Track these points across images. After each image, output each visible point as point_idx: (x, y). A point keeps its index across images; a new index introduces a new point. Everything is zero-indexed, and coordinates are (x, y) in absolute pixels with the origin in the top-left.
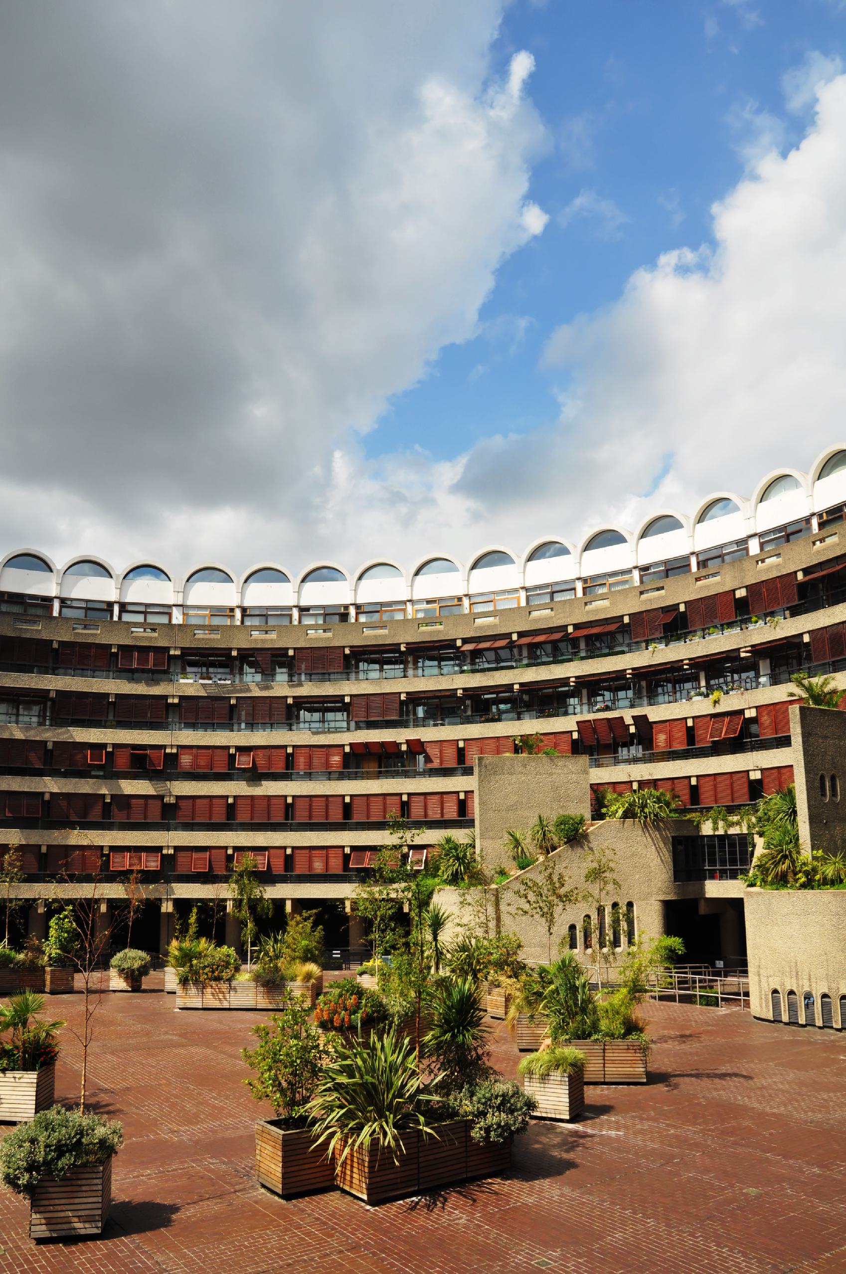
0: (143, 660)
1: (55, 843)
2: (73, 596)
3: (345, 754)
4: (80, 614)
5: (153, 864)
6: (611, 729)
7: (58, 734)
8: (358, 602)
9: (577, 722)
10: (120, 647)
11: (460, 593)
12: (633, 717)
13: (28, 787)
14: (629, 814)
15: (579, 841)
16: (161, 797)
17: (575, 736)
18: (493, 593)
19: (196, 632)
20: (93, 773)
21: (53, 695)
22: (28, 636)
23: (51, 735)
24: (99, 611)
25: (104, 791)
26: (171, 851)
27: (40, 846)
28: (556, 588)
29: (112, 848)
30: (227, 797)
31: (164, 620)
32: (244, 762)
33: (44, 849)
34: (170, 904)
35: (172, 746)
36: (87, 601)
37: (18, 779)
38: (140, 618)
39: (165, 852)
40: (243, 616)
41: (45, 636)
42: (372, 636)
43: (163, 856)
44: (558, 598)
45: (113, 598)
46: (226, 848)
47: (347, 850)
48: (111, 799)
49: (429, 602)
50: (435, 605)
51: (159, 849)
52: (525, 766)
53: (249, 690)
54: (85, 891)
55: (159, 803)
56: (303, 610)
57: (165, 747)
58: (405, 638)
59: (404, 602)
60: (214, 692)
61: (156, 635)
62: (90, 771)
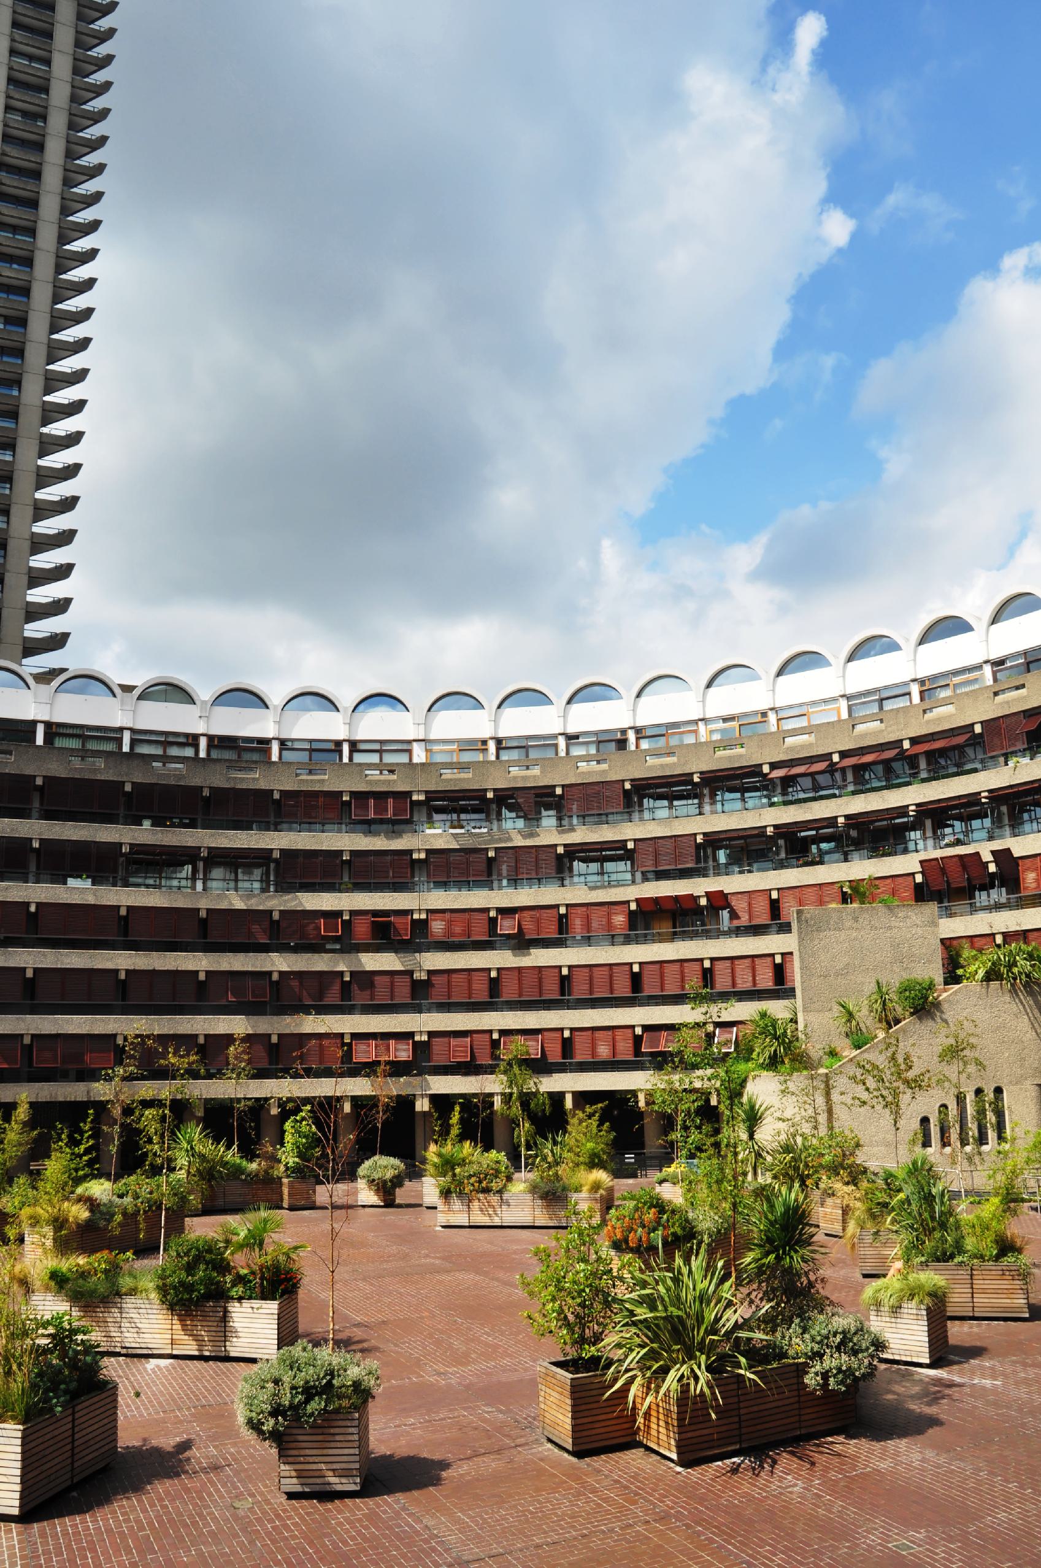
0: (381, 809)
1: (287, 1031)
2: (294, 736)
3: (631, 913)
4: (304, 757)
5: (404, 1053)
6: (964, 867)
9: (921, 862)
10: (353, 794)
11: (763, 706)
12: (993, 852)
14: (992, 975)
15: (929, 1011)
17: (919, 878)
19: (442, 771)
20: (328, 946)
21: (276, 855)
23: (277, 903)
24: (326, 751)
25: (342, 967)
26: (425, 1038)
27: (269, 1035)
28: (885, 694)
29: (355, 1036)
30: (489, 970)
31: (403, 759)
32: (507, 927)
33: (274, 1039)
34: (426, 1101)
36: (311, 741)
38: (374, 758)
39: (417, 1038)
40: (499, 749)
41: (263, 785)
42: (656, 766)
43: (415, 1043)
44: (888, 706)
45: (340, 737)
46: (490, 1032)
47: (639, 1031)
49: (725, 720)
50: (735, 724)
51: (410, 1035)
52: (856, 919)
53: (510, 839)
54: (324, 1087)
55: (407, 979)
56: (571, 738)
57: (411, 912)
59: (696, 722)
60: (469, 843)
61: (395, 777)
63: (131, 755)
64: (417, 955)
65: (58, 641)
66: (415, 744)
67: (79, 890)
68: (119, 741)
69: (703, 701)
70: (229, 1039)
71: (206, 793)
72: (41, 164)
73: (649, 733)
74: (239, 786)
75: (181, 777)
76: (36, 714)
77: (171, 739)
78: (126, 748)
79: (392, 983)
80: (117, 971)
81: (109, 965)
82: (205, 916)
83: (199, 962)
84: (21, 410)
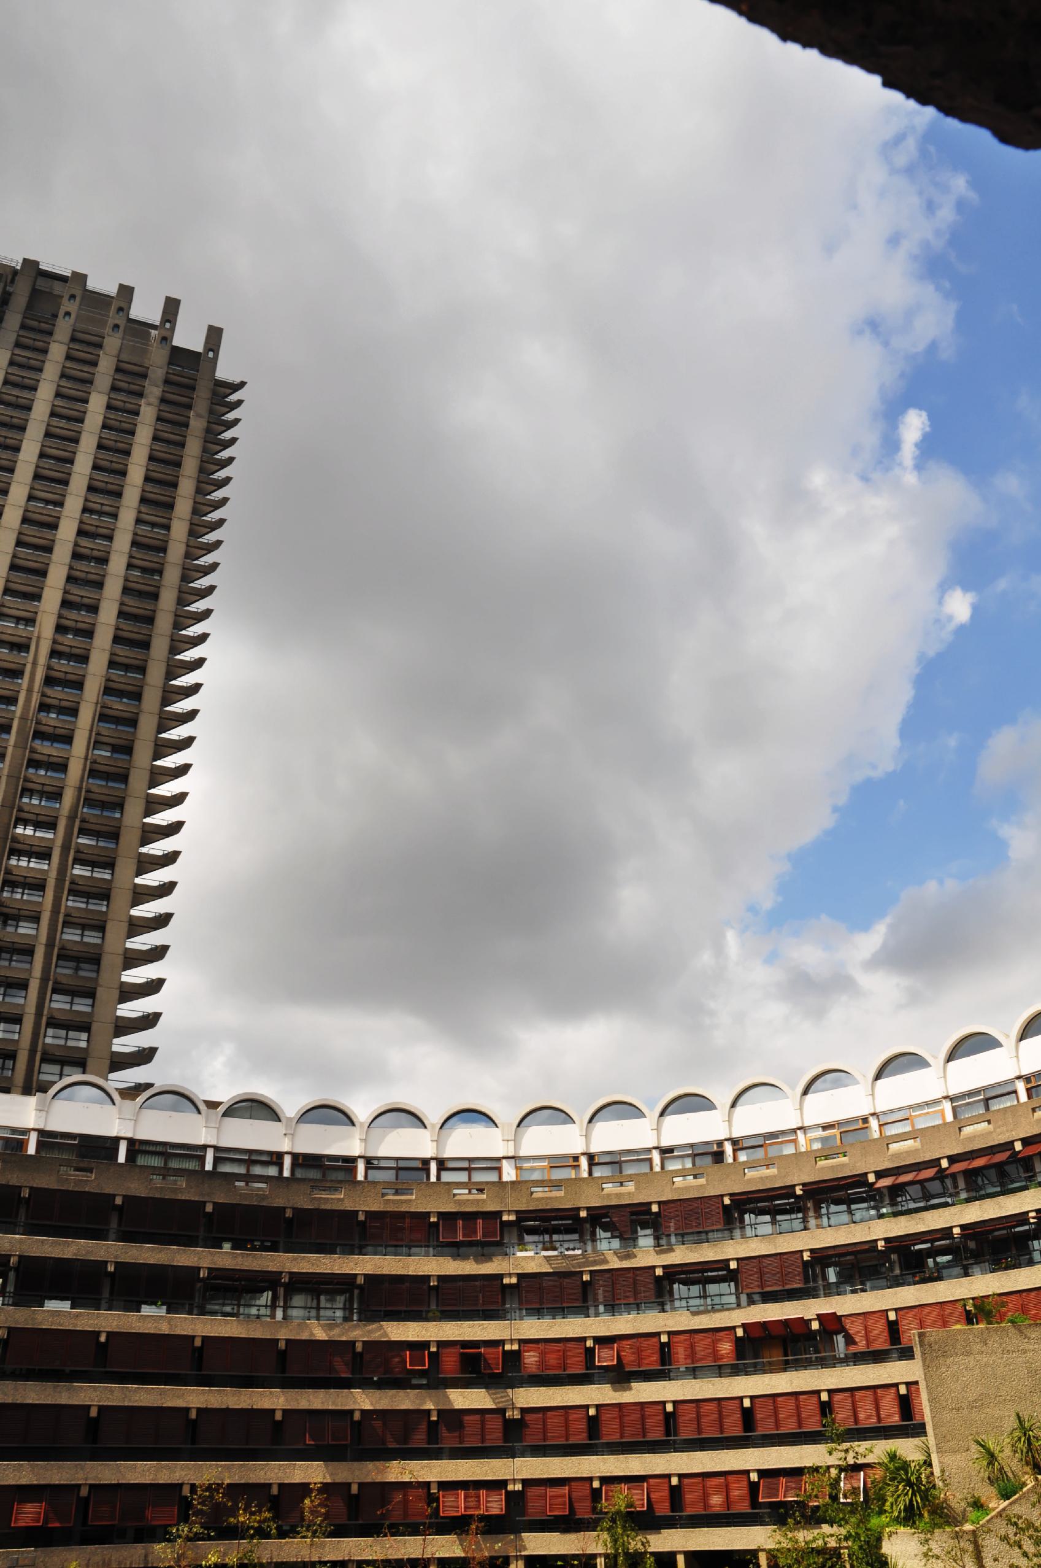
0: (470, 1230)
2: (380, 1154)
3: (738, 1339)
4: (389, 1176)
5: (495, 1505)
7: (369, 1331)
8: (734, 1136)
10: (440, 1214)
11: (865, 1111)
13: (333, 1403)
16: (503, 1411)
18: (910, 1107)
19: (533, 1189)
20: (415, 1382)
21: (360, 1280)
22: (328, 1207)
23: (360, 1333)
24: (412, 1170)
26: (518, 1487)
27: (349, 1484)
29: (444, 1485)
30: (587, 1407)
31: (492, 1177)
32: (605, 1358)
33: (355, 1489)
35: (512, 1341)
36: (397, 1159)
37: (322, 1393)
38: (462, 1177)
39: (510, 1487)
41: (348, 1206)
43: (508, 1493)
44: (995, 1105)
46: (590, 1479)
48: (438, 1416)
49: (826, 1127)
51: (503, 1484)
53: (605, 1261)
55: (498, 1418)
57: (502, 1342)
58: (799, 1177)
59: (794, 1131)
60: (562, 1266)
61: (484, 1196)
62: (410, 1379)
63: (214, 1173)
64: (509, 1390)
65: (145, 1056)
66: (504, 1161)
67: (152, 1318)
68: (202, 1159)
69: (801, 1109)
70: (304, 1489)
71: (289, 1214)
72: (154, 611)
73: (746, 1144)
74: (323, 1207)
75: (264, 1197)
76: (119, 1130)
77: (254, 1157)
78: (209, 1167)
79: (483, 1423)
80: (188, 1409)
81: (180, 1403)
82: (283, 1347)
83: (274, 1400)
84: (123, 831)
